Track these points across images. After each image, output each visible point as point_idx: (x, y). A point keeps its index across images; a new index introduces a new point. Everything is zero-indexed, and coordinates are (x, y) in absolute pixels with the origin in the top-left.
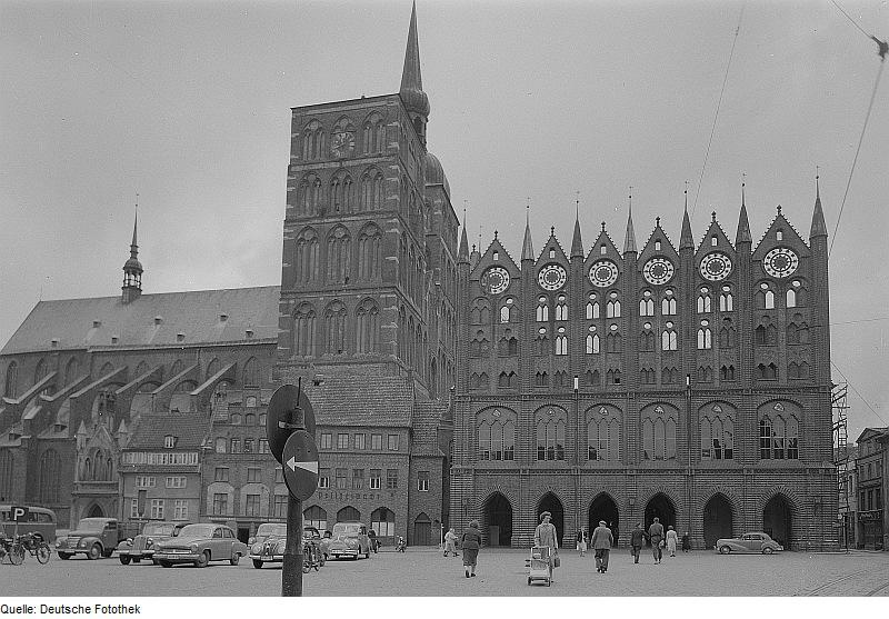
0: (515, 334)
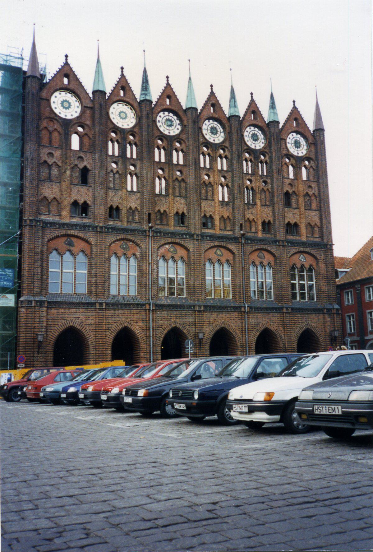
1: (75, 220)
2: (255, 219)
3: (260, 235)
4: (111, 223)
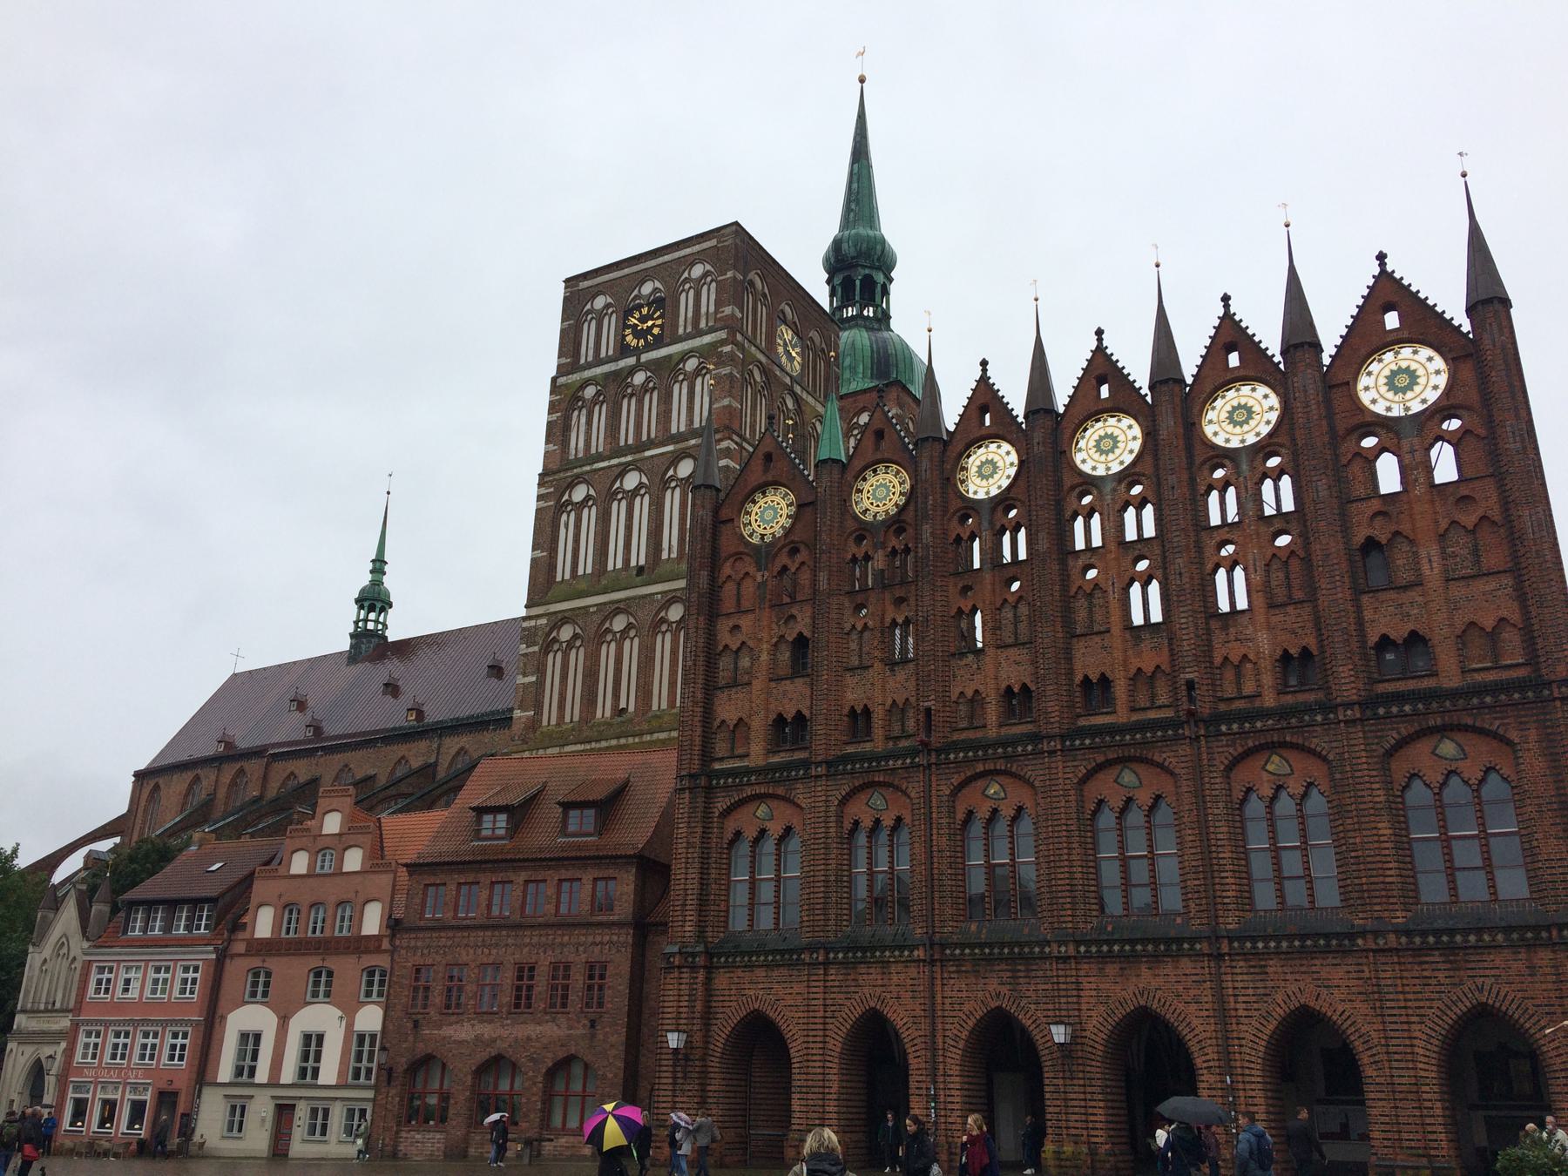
0: (803, 625)
1: (776, 759)
2: (1251, 656)
3: (1269, 700)
4: (850, 749)
